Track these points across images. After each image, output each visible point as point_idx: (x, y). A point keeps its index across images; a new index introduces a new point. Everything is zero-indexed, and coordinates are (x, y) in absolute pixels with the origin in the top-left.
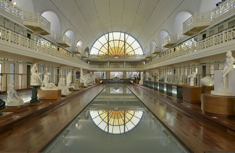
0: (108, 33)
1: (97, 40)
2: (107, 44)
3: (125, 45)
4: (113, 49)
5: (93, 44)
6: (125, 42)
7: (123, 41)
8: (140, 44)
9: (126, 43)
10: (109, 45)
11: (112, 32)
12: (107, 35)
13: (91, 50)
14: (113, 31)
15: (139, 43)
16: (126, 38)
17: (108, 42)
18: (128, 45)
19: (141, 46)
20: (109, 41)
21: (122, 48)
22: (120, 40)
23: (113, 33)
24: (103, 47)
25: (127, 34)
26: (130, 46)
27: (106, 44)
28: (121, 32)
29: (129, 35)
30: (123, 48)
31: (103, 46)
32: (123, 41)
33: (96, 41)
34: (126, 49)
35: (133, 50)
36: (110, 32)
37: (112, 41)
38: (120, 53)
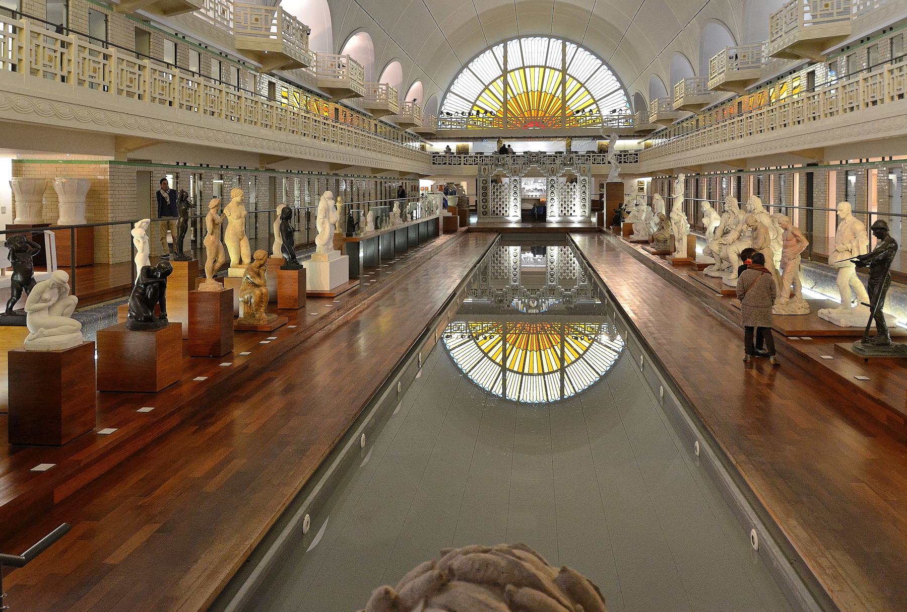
0: (505, 42)
1: (466, 66)
2: (500, 82)
3: (563, 82)
4: (521, 98)
5: (452, 83)
6: (564, 71)
7: (558, 70)
8: (619, 80)
9: (570, 76)
10: (506, 83)
11: (519, 38)
12: (499, 50)
13: (442, 104)
14: (521, 33)
15: (615, 74)
16: (567, 57)
17: (505, 72)
18: (575, 82)
19: (623, 87)
20: (509, 70)
21: (554, 96)
22: (545, 67)
23: (523, 40)
24: (487, 91)
25: (572, 42)
26: (582, 85)
27: (498, 81)
28: (550, 37)
29: (579, 45)
30: (557, 95)
31: (487, 87)
32: (558, 70)
33: (461, 71)
34: (567, 99)
35: (595, 102)
36: (511, 39)
37: (517, 72)
38: (546, 112)
